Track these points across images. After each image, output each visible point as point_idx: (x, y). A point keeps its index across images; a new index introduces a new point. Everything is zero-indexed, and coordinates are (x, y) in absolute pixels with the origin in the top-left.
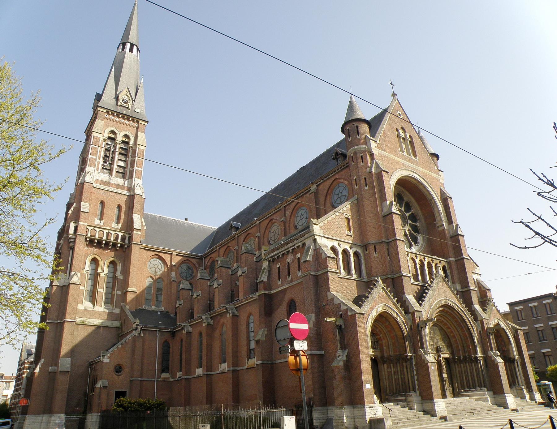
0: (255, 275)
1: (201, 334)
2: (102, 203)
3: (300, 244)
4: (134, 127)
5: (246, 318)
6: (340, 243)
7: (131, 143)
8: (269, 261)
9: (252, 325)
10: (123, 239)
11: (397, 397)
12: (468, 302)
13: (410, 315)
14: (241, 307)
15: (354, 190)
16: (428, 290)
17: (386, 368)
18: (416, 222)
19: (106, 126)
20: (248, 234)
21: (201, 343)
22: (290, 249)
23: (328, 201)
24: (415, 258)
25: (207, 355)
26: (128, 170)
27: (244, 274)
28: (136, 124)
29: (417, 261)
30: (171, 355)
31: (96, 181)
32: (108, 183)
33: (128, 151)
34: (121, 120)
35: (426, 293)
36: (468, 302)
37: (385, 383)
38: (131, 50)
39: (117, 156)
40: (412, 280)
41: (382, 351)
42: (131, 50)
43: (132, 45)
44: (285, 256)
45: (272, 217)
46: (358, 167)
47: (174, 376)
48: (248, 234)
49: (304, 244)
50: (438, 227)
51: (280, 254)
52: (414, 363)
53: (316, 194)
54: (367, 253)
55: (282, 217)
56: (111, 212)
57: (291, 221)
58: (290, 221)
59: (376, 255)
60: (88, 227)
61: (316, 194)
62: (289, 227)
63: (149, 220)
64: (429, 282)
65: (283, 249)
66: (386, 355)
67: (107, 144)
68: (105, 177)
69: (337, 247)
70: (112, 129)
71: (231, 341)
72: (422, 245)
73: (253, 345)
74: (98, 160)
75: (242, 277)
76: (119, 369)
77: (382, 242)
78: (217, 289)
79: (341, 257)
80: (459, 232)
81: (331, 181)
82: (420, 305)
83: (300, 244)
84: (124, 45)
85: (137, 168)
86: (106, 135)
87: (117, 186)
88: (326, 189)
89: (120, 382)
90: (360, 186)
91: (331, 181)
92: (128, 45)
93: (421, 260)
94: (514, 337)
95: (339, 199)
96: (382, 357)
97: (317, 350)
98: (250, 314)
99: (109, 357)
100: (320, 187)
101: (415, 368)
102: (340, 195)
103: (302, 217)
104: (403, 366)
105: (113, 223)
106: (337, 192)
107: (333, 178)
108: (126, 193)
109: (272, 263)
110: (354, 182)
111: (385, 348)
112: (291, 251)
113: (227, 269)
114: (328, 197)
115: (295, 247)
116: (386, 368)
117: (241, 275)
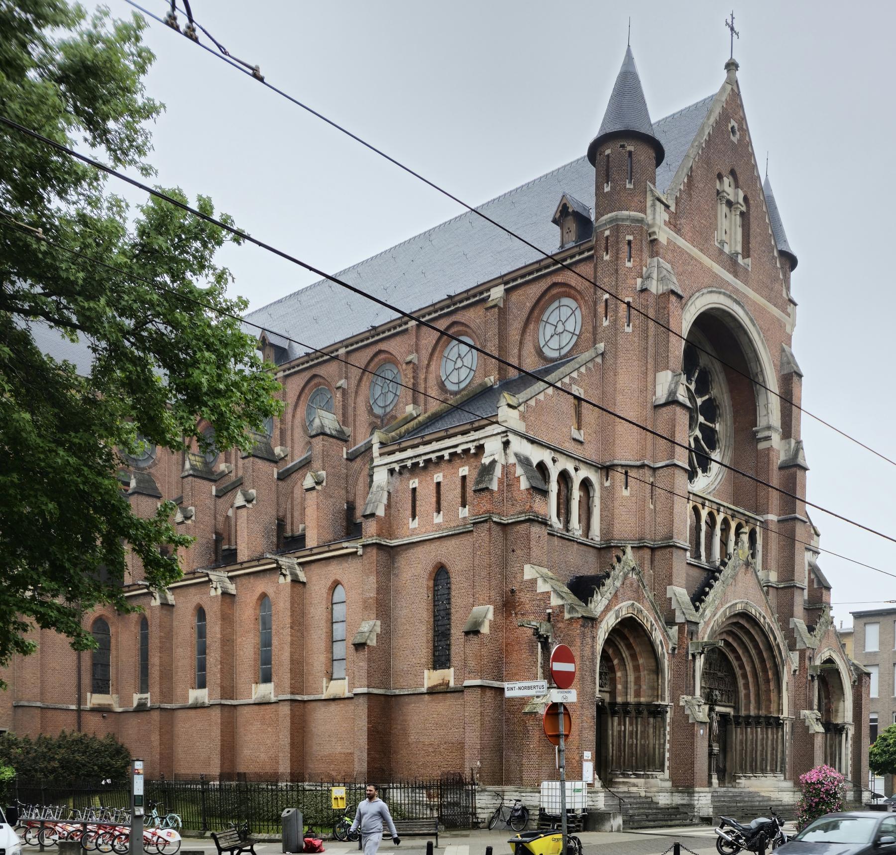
0: (344, 492)
1: (201, 613)
3: (470, 445)
5: (324, 591)
6: (557, 456)
8: (392, 471)
9: (339, 611)
11: (628, 776)
12: (785, 614)
13: (676, 628)
14: (313, 567)
15: (600, 330)
16: (716, 579)
17: (615, 724)
18: (713, 422)
20: (315, 376)
21: (202, 633)
22: (446, 454)
23: (528, 338)
24: (700, 506)
25: (221, 663)
27: (318, 488)
29: (704, 514)
30: (113, 652)
35: (711, 587)
36: (785, 614)
37: (612, 750)
40: (688, 554)
41: (613, 693)
44: (431, 467)
45: (383, 346)
46: (617, 271)
47: (124, 699)
48: (315, 376)
49: (480, 449)
50: (760, 440)
51: (421, 460)
52: (668, 720)
53: (502, 312)
54: (607, 484)
55: (411, 352)
57: (433, 367)
58: (428, 365)
59: (626, 493)
61: (502, 312)
62: (426, 379)
64: (718, 563)
65: (428, 448)
66: (619, 700)
69: (549, 463)
71: (289, 639)
72: (717, 475)
73: (339, 650)
75: (314, 493)
77: (643, 466)
78: (243, 512)
79: (554, 487)
80: (800, 461)
81: (543, 285)
82: (697, 609)
83: (470, 445)
88: (529, 305)
90: (615, 322)
91: (543, 285)
93: (711, 514)
94: (853, 686)
95: (556, 337)
96: (613, 704)
97: (494, 679)
98: (336, 584)
100: (514, 297)
101: (668, 729)
102: (560, 328)
103: (459, 364)
104: (648, 724)
106: (553, 319)
107: (549, 281)
109: (396, 475)
110: (601, 309)
111: (619, 687)
112: (447, 457)
113: (267, 464)
114: (531, 326)
115: (459, 450)
116: (615, 724)
117: (313, 489)
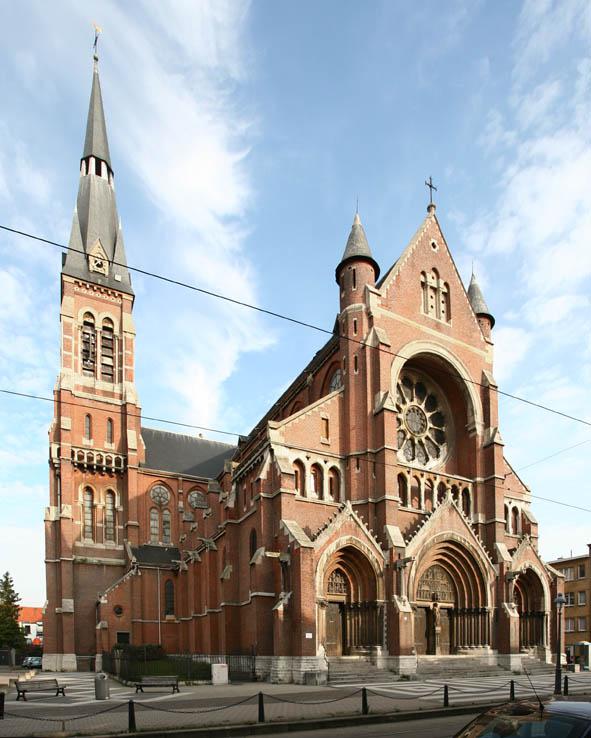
2: (89, 416)
4: (117, 305)
7: (116, 331)
10: (118, 462)
19: (78, 306)
26: (116, 370)
28: (119, 301)
31: (77, 388)
32: (92, 390)
33: (112, 340)
34: (105, 296)
38: (98, 172)
39: (99, 351)
42: (98, 172)
43: (98, 162)
56: (101, 427)
60: (74, 449)
63: (147, 435)
67: (84, 333)
68: (88, 381)
70: (88, 310)
74: (74, 357)
76: (118, 610)
84: (87, 159)
85: (128, 367)
86: (81, 320)
87: (106, 393)
89: (122, 623)
92: (92, 161)
99: (106, 598)
105: (106, 443)
108: (119, 402)
